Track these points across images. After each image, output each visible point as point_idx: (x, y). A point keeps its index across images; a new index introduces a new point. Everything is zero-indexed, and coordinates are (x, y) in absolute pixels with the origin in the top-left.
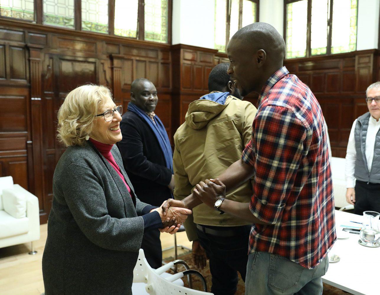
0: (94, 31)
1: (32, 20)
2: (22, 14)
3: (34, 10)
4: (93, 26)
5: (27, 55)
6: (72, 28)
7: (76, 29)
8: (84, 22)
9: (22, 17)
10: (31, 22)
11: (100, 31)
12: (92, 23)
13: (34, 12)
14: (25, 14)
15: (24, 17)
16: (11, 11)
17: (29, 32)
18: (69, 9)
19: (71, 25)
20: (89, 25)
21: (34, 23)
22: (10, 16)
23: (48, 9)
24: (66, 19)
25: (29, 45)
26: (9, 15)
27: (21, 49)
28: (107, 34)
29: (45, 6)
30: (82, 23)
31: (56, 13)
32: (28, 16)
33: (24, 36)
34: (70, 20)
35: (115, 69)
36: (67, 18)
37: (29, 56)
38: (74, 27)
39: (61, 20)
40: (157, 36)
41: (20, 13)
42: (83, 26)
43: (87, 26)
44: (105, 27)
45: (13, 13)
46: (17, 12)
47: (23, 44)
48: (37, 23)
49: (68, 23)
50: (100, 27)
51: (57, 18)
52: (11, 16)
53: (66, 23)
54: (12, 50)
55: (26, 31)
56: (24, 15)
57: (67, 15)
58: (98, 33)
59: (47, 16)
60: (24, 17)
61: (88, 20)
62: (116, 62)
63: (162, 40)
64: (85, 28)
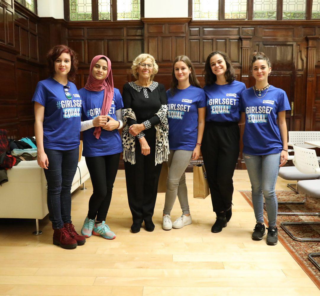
0: (293, 18)
1: (245, 18)
2: (239, 15)
3: (247, 11)
4: (292, 15)
5: (240, 44)
6: (274, 19)
7: (277, 20)
8: (285, 13)
9: (239, 18)
10: (244, 19)
11: (298, 18)
12: (291, 12)
13: (247, 12)
14: (240, 14)
15: (239, 17)
16: (232, 14)
17: (242, 28)
18: (273, 4)
19: (274, 17)
20: (289, 15)
21: (246, 20)
22: (231, 18)
23: (257, 8)
24: (270, 13)
25: (242, 36)
26: (230, 18)
27: (237, 40)
29: (254, 5)
30: (283, 13)
31: (263, 10)
32: (243, 15)
33: (239, 31)
34: (273, 13)
35: (309, 48)
36: (270, 12)
37: (242, 45)
38: (276, 18)
39: (266, 14)
41: (237, 14)
42: (284, 16)
43: (287, 16)
44: (303, 14)
45: (232, 15)
46: (236, 14)
47: (237, 37)
48: (248, 20)
49: (272, 16)
51: (263, 13)
52: (231, 17)
53: (270, 16)
54: (230, 42)
55: (241, 27)
56: (240, 15)
57: (271, 10)
58: (297, 20)
59: (256, 13)
60: (239, 17)
61: (288, 10)
62: (310, 43)
64: (286, 18)
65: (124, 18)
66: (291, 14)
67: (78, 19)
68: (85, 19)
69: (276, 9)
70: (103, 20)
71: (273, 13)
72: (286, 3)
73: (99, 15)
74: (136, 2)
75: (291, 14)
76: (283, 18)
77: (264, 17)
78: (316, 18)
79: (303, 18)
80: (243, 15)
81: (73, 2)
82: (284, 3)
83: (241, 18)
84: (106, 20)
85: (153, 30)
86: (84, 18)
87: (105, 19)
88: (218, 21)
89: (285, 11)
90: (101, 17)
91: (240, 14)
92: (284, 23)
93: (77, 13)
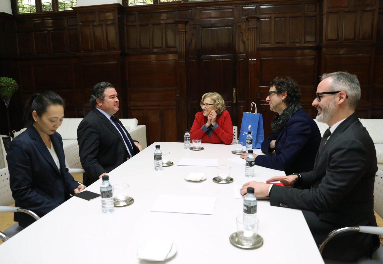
21: (183, 2)
22: (166, 1)
65: (64, 8)
67: (24, 12)
68: (30, 12)
70: (47, 12)
73: (43, 7)
84: (49, 11)
86: (29, 11)
87: (48, 10)
88: (153, 5)
92: (221, 3)
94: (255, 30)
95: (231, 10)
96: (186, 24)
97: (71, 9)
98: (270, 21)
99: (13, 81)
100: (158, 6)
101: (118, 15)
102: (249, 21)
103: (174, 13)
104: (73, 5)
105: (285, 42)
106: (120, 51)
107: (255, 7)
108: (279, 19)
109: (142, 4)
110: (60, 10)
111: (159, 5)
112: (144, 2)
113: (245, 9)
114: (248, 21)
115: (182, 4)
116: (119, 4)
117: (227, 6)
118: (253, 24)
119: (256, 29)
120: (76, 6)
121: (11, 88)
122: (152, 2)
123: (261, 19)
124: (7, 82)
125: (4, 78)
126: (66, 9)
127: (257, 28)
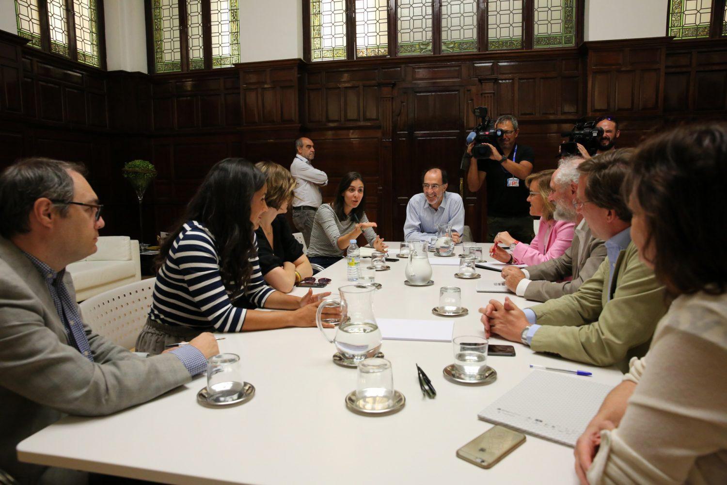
1: (387, 54)
2: (377, 51)
7: (434, 54)
8: (445, 43)
10: (385, 56)
11: (465, 49)
14: (379, 49)
16: (367, 49)
19: (430, 50)
20: (452, 46)
21: (389, 57)
22: (366, 56)
26: (365, 55)
28: (476, 52)
34: (428, 44)
39: (417, 47)
40: (556, 38)
42: (444, 48)
43: (448, 48)
45: (368, 51)
49: (426, 48)
50: (466, 44)
51: (412, 46)
53: (422, 49)
56: (378, 50)
57: (424, 40)
58: (464, 52)
63: (565, 43)
65: (221, 65)
66: (455, 44)
67: (164, 70)
68: (173, 70)
69: (431, 38)
70: (196, 70)
71: (428, 44)
72: (447, 29)
74: (235, 42)
75: (455, 44)
76: (443, 51)
77: (413, 52)
78: (496, 48)
79: (473, 49)
80: (383, 51)
81: (158, 48)
82: (443, 29)
83: (380, 54)
85: (253, 78)
87: (197, 68)
89: (445, 41)
90: (192, 65)
91: (378, 48)
93: (164, 62)
94: (491, 97)
95: (457, 68)
96: (393, 88)
97: (229, 66)
98: (513, 84)
99: (151, 166)
100: (353, 61)
101: (298, 74)
102: (483, 84)
103: (376, 71)
104: (234, 60)
105: (534, 114)
106: (300, 125)
107: (491, 64)
108: (525, 81)
109: (331, 59)
110: (215, 67)
111: (355, 61)
112: (334, 57)
113: (477, 67)
114: (481, 83)
115: (389, 59)
116: (300, 60)
117: (451, 63)
118: (489, 88)
119: (492, 95)
120: (237, 62)
121: (149, 175)
122: (345, 56)
123: (500, 81)
124: (143, 167)
125: (140, 161)
126: (223, 67)
127: (494, 93)
